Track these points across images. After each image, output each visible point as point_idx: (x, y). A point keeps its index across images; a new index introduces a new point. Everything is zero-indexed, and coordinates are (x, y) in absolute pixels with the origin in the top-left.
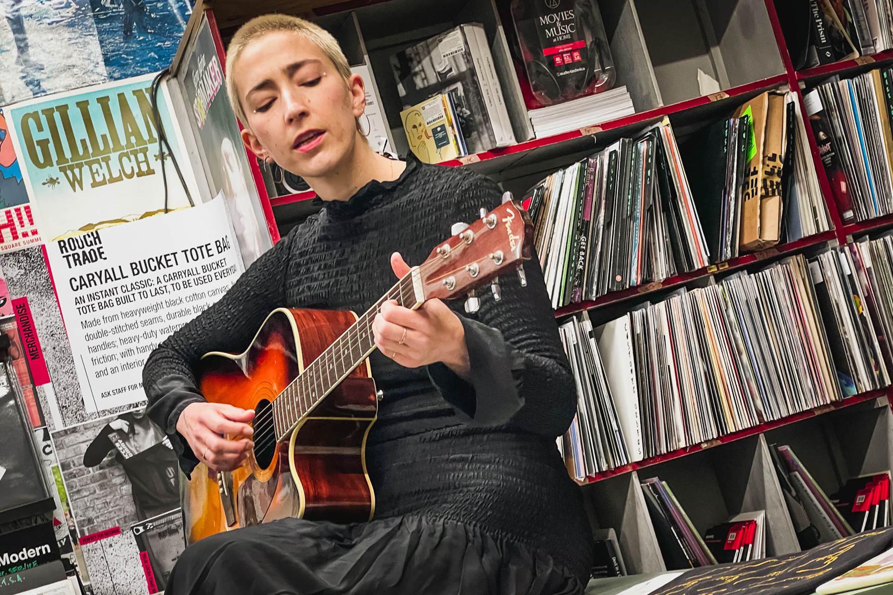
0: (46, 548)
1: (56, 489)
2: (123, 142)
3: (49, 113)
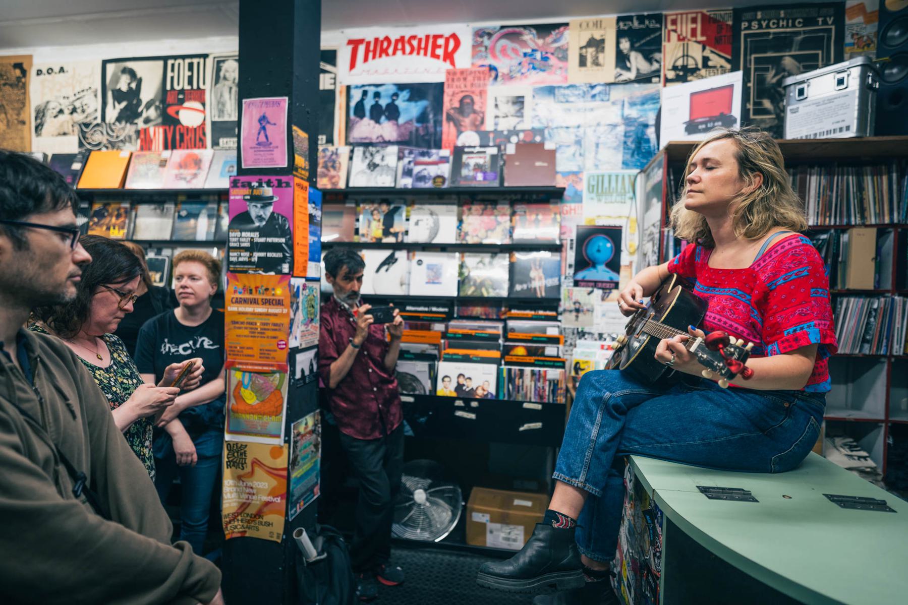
0: (554, 313)
1: (562, 297)
2: (619, 190)
3: (598, 176)
